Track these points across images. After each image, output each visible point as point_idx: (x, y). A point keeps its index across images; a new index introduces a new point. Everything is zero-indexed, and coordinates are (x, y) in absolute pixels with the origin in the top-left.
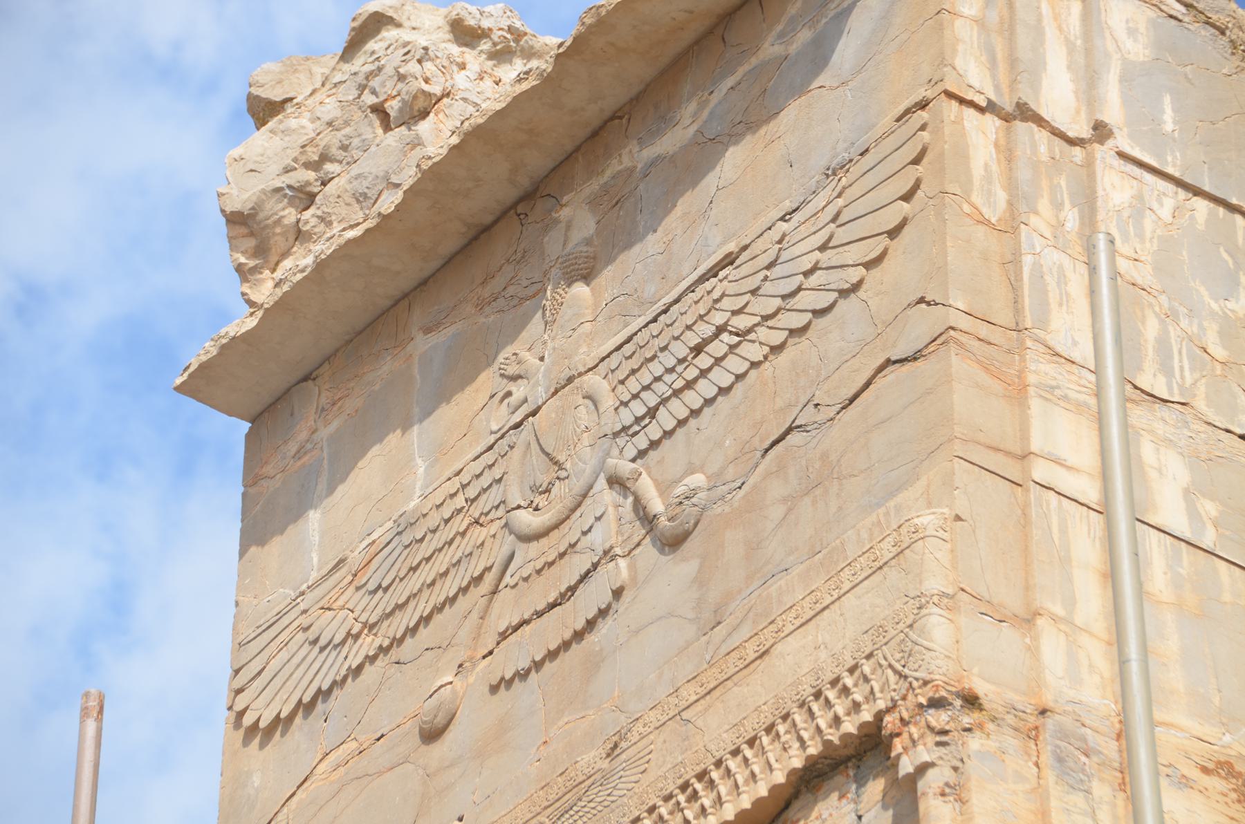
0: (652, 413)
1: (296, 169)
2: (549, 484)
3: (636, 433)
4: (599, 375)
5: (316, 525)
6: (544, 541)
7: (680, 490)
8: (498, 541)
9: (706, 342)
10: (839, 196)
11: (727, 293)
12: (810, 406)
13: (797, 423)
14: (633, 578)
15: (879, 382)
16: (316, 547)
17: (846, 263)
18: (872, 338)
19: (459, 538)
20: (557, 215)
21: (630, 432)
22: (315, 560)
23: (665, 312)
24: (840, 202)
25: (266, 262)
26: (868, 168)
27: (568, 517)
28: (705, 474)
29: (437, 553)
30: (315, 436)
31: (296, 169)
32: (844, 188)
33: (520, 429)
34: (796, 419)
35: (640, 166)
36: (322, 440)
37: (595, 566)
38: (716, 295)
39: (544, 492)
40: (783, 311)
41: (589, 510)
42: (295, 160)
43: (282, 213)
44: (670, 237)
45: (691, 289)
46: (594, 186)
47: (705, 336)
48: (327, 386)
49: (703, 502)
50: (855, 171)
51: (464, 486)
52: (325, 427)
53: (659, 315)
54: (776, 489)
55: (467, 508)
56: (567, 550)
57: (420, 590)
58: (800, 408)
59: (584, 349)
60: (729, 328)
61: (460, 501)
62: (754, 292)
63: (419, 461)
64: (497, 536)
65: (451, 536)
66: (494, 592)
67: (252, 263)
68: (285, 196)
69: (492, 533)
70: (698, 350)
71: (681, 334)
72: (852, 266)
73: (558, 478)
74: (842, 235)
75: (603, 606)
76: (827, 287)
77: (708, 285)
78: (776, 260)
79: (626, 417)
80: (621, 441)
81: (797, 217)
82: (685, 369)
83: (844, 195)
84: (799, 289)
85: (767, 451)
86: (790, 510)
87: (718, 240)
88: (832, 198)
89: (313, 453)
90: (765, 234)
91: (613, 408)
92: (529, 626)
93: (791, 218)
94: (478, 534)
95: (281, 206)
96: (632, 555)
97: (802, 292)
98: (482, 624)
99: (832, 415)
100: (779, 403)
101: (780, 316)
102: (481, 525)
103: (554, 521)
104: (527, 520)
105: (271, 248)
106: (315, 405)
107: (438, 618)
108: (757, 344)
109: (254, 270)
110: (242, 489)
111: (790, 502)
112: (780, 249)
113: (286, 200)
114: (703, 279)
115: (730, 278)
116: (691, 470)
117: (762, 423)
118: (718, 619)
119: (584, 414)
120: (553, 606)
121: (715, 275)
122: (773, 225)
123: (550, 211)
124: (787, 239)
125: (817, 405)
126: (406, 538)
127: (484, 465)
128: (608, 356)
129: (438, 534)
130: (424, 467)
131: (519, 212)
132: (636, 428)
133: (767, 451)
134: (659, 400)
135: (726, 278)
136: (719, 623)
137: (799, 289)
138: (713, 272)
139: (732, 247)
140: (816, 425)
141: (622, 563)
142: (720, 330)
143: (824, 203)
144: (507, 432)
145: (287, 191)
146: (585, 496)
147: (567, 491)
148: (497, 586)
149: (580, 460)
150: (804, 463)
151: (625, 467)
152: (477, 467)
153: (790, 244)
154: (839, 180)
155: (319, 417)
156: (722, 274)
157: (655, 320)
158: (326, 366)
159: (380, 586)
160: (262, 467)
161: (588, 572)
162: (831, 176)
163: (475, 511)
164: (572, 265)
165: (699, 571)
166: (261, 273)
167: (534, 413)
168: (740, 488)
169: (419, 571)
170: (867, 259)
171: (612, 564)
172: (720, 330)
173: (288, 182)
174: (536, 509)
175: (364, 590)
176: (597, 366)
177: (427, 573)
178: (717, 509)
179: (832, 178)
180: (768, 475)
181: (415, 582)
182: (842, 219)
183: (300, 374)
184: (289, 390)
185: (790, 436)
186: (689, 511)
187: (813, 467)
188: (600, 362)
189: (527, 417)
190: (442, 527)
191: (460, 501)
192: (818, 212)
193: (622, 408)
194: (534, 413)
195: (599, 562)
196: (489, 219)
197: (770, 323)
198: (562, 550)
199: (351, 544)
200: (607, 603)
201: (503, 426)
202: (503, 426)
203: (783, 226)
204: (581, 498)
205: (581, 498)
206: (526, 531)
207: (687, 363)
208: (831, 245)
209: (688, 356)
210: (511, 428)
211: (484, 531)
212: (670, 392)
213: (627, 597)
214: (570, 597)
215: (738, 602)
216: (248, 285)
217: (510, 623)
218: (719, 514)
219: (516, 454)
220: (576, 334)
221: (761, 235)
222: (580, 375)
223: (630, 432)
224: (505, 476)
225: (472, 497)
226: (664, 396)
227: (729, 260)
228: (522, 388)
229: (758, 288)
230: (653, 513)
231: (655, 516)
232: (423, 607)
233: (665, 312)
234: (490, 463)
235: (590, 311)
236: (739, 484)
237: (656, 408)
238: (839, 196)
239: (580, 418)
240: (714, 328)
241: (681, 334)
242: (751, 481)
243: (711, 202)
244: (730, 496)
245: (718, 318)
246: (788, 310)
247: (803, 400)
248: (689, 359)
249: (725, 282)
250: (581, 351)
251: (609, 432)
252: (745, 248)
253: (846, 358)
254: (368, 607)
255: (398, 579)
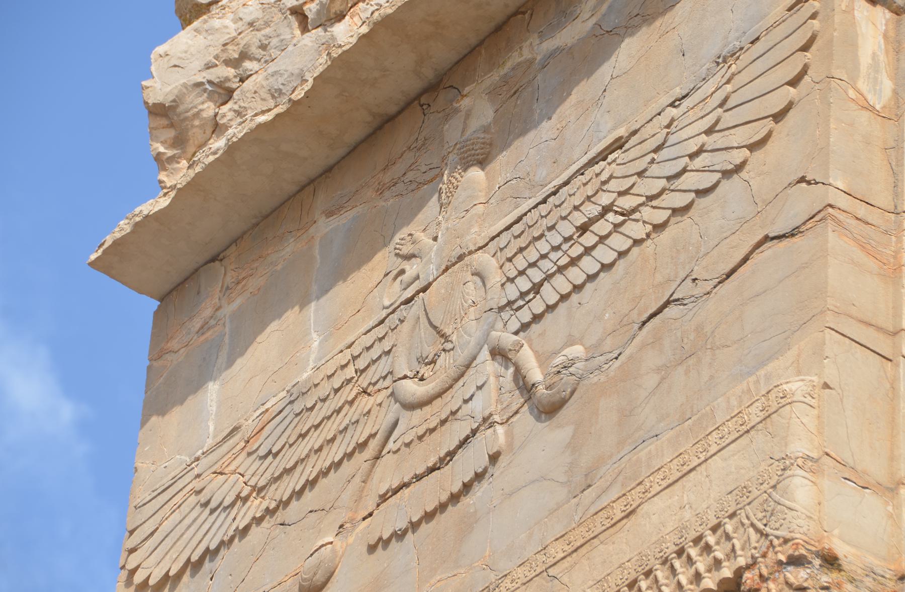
0: (536, 288)
1: (216, 66)
2: (435, 355)
3: (520, 308)
4: (488, 254)
5: (214, 396)
6: (427, 409)
7: (559, 360)
8: (383, 410)
9: (592, 221)
10: (728, 82)
11: (615, 175)
12: (689, 281)
13: (675, 296)
14: (510, 444)
15: (757, 257)
16: (213, 417)
17: (731, 146)
18: (751, 216)
19: (347, 407)
20: (458, 105)
21: (515, 306)
22: (212, 428)
23: (554, 193)
24: (729, 88)
25: (184, 152)
26: (758, 55)
27: (451, 387)
28: (583, 345)
29: (325, 421)
30: (219, 313)
31: (216, 66)
32: (733, 75)
33: (411, 304)
34: (674, 293)
35: (539, 58)
36: (225, 316)
37: (474, 432)
38: (604, 177)
39: (430, 363)
40: (667, 192)
41: (471, 379)
42: (217, 57)
43: (201, 107)
44: (564, 123)
45: (580, 172)
46: (495, 77)
47: (591, 216)
48: (233, 267)
49: (581, 372)
50: (745, 58)
51: (355, 358)
52: (229, 304)
53: (549, 196)
54: (652, 359)
55: (356, 378)
56: (448, 417)
57: (308, 456)
58: (678, 283)
59: (476, 229)
60: (615, 208)
61: (350, 372)
62: (640, 174)
63: (314, 335)
64: (383, 405)
65: (340, 405)
66: (377, 458)
67: (170, 153)
68: (205, 90)
69: (379, 401)
70: (583, 229)
71: (569, 214)
72: (737, 148)
73: (444, 350)
74: (729, 119)
75: (480, 470)
76: (711, 168)
77: (597, 168)
78: (663, 144)
79: (512, 292)
80: (505, 315)
81: (687, 103)
82: (570, 247)
83: (732, 81)
84: (684, 171)
85: (644, 323)
86: (663, 379)
87: (609, 126)
88: (720, 85)
89: (216, 329)
90: (654, 120)
91: (499, 284)
92: (408, 489)
93: (680, 104)
94: (366, 403)
95: (200, 99)
96: (510, 422)
97: (686, 174)
98: (364, 487)
99: (709, 289)
100: (659, 278)
101: (664, 196)
102: (369, 395)
103: (437, 389)
104: (412, 389)
105: (189, 140)
106: (220, 284)
107: (322, 482)
108: (641, 223)
109: (172, 159)
110: (148, 363)
111: (665, 372)
112: (668, 134)
113: (206, 95)
114: (592, 162)
115: (618, 161)
116: (571, 342)
117: (641, 297)
118: (589, 482)
119: (472, 290)
120: (432, 470)
121: (604, 159)
122: (663, 110)
123: (452, 101)
124: (675, 124)
125: (694, 280)
126: (297, 407)
127: (375, 337)
128: (498, 235)
129: (327, 403)
130: (318, 341)
131: (422, 103)
132: (521, 303)
133: (644, 323)
134: (544, 276)
135: (614, 161)
136: (590, 486)
137: (684, 171)
138: (602, 156)
139: (622, 132)
140: (693, 299)
141: (500, 430)
142: (606, 210)
143: (713, 89)
144: (399, 307)
145: (207, 86)
146: (468, 366)
147: (452, 361)
148: (381, 451)
149: (465, 333)
150: (679, 334)
151: (508, 339)
152: (368, 340)
153: (678, 128)
154: (729, 67)
155: (224, 295)
156: (611, 158)
157: (544, 201)
158: (233, 247)
159: (270, 452)
160: (168, 342)
161: (467, 438)
162: (721, 63)
163: (364, 382)
164: (469, 150)
165: (573, 436)
166: (179, 163)
167: (424, 290)
168: (616, 358)
169: (307, 438)
170: (752, 141)
171: (491, 430)
172: (606, 210)
173: (209, 77)
174: (422, 379)
175: (255, 456)
176: (487, 244)
177: (315, 440)
178: (594, 379)
179: (721, 66)
180: (643, 346)
181: (303, 448)
182: (730, 104)
183: (207, 256)
184: (197, 270)
185: (667, 309)
186: (567, 380)
187: (688, 338)
188: (490, 241)
189: (418, 292)
190: (331, 396)
191: (350, 372)
192: (707, 97)
193: (508, 284)
194: (424, 290)
195: (478, 429)
196: (393, 109)
197: (654, 203)
198: (443, 417)
199: (246, 413)
200: (483, 467)
201: (395, 302)
202: (395, 302)
203: (673, 112)
204: (464, 369)
205: (464, 369)
206: (410, 399)
207: (573, 242)
208: (717, 128)
209: (574, 234)
210: (402, 304)
211: (371, 400)
212: (555, 268)
213: (503, 461)
214: (449, 462)
215: (608, 466)
216: (165, 173)
217: (390, 486)
218: (595, 384)
219: (406, 327)
220: (469, 215)
221: (651, 120)
222: (470, 253)
223: (515, 306)
224: (394, 348)
225: (362, 368)
226: (549, 273)
227: (619, 144)
228: (415, 267)
229: (645, 170)
230: (532, 382)
231: (533, 385)
232: (309, 471)
233: (554, 193)
234: (380, 336)
235: (483, 194)
236: (616, 355)
237: (541, 284)
238: (728, 82)
239: (468, 294)
240: (600, 208)
241: (569, 214)
242: (628, 352)
243: (605, 91)
244: (607, 366)
245: (605, 199)
246: (673, 191)
247: (682, 275)
248: (575, 237)
249: (613, 165)
250: (473, 231)
251: (495, 306)
252: (635, 133)
253: (725, 235)
254: (258, 472)
255: (287, 446)
